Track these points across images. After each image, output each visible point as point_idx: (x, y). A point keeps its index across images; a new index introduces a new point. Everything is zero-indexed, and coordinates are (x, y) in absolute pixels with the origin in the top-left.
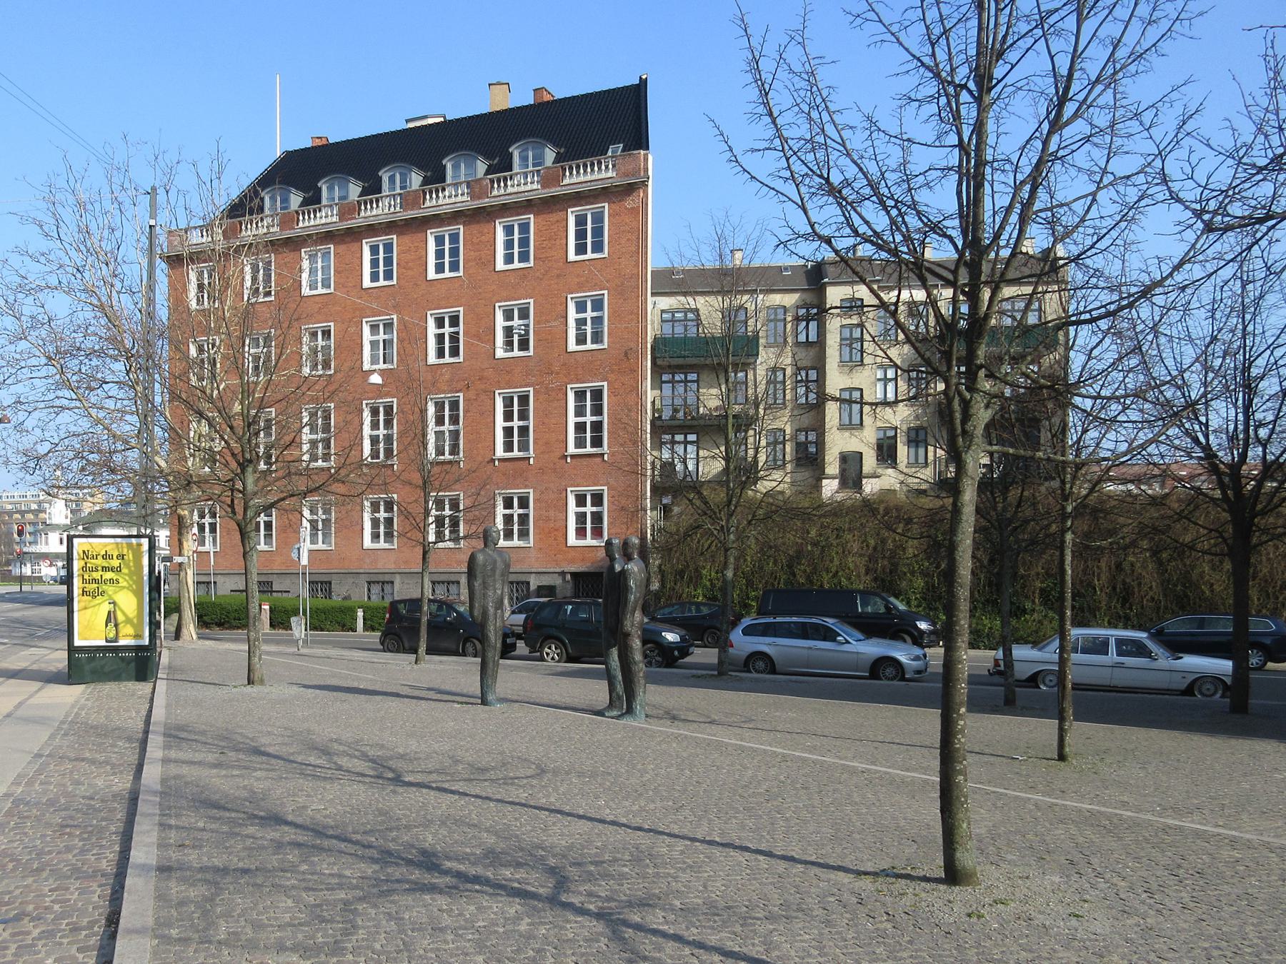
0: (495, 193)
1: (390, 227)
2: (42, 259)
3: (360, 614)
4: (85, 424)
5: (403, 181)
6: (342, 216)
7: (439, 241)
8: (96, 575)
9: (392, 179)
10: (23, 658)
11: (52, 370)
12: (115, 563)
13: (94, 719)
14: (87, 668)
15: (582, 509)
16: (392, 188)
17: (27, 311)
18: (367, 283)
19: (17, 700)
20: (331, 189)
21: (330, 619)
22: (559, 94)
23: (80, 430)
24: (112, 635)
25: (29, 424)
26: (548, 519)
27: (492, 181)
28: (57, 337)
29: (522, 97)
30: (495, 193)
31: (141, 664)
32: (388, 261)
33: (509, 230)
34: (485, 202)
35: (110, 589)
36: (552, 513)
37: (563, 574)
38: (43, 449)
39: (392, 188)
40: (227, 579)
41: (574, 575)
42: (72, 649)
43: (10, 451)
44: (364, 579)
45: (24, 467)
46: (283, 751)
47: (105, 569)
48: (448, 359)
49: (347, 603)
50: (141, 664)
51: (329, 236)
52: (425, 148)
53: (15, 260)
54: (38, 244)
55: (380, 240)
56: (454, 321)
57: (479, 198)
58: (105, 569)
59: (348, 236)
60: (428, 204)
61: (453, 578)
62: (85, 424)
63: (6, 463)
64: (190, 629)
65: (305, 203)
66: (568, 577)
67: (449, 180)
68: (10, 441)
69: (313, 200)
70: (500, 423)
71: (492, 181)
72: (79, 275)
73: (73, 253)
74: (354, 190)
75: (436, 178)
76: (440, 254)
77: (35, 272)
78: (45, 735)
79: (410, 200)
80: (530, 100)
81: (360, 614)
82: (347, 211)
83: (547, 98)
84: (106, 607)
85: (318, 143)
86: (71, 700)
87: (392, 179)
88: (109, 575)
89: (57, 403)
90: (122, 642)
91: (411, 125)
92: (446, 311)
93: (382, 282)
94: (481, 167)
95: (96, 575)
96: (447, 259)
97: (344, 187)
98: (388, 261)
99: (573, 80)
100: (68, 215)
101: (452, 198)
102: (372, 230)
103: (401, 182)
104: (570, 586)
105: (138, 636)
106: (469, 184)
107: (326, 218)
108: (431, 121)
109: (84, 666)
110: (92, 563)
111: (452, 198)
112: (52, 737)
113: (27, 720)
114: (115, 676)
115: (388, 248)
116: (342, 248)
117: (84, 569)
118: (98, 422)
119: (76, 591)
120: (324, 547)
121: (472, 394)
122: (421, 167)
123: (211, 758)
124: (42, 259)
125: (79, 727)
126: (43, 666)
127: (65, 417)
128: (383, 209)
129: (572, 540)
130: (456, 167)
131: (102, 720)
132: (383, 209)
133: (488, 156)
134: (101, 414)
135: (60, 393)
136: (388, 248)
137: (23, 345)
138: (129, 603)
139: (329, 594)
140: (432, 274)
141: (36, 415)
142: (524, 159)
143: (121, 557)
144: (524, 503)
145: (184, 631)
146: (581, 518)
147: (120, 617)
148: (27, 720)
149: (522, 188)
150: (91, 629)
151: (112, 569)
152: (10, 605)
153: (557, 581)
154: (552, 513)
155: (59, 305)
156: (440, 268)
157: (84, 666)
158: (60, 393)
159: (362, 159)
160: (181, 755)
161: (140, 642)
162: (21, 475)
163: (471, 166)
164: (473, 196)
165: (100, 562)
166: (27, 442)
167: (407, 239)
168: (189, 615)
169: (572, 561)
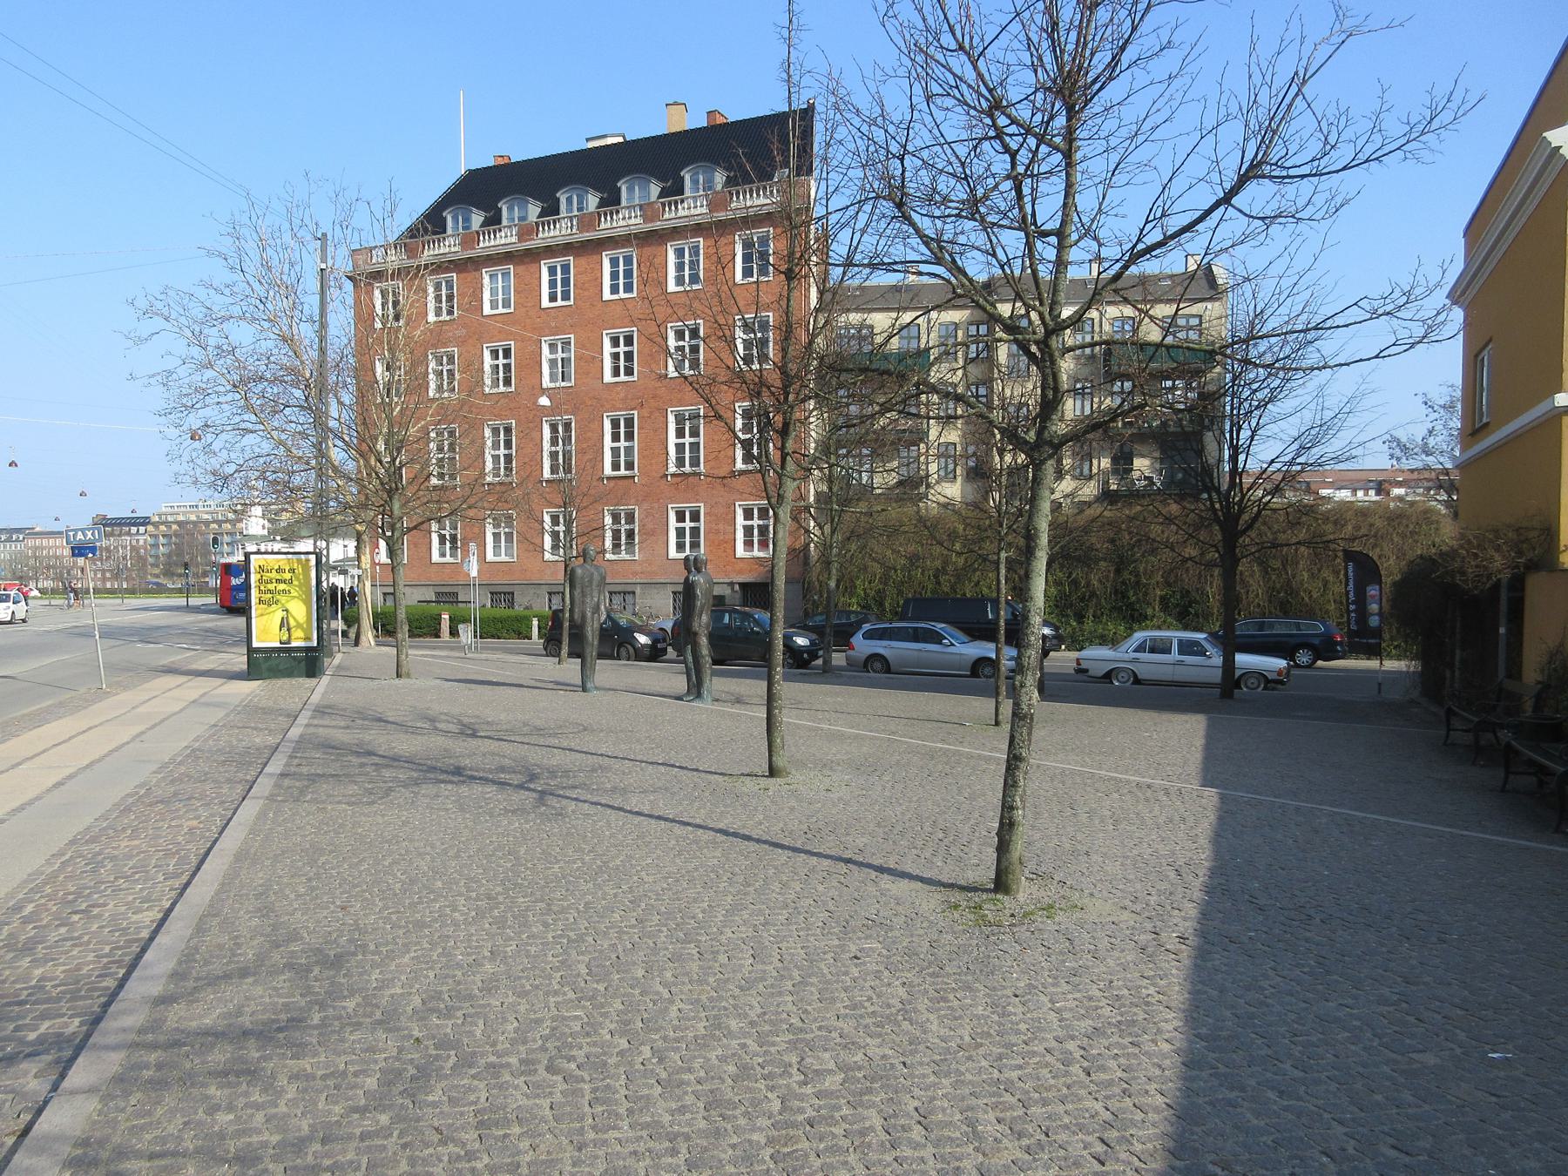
0: (667, 216)
1: (567, 248)
2: (227, 291)
3: (535, 622)
4: (266, 447)
5: (580, 202)
6: (522, 236)
7: (614, 262)
8: (271, 587)
9: (569, 200)
10: (212, 661)
11: (238, 396)
12: (287, 576)
13: (263, 704)
14: (264, 666)
15: (749, 523)
16: (570, 210)
17: (212, 342)
18: (545, 303)
19: (202, 691)
20: (510, 209)
21: (501, 626)
22: (733, 117)
23: (264, 452)
24: (285, 638)
25: (216, 446)
26: (718, 532)
27: (663, 205)
28: (241, 366)
29: (696, 120)
30: (667, 216)
31: (309, 662)
32: (566, 282)
33: (680, 253)
34: (657, 225)
35: (283, 598)
36: (721, 526)
37: (731, 584)
38: (231, 469)
39: (570, 210)
40: (415, 590)
41: (743, 585)
42: (251, 651)
43: (199, 471)
44: (545, 590)
45: (213, 485)
46: (398, 720)
47: (278, 581)
48: (623, 378)
49: (527, 613)
50: (309, 662)
51: (507, 257)
52: (601, 169)
53: (201, 293)
54: (222, 276)
55: (558, 261)
56: (629, 341)
57: (652, 221)
58: (278, 581)
59: (527, 257)
60: (603, 226)
61: (629, 588)
62: (266, 447)
63: (195, 482)
64: (368, 636)
65: (486, 223)
66: (737, 587)
67: (624, 203)
68: (199, 462)
69: (493, 221)
70: (672, 439)
71: (663, 205)
72: (261, 307)
73: (256, 286)
74: (534, 210)
75: (611, 201)
76: (614, 276)
77: (219, 303)
78: (221, 714)
79: (587, 222)
80: (702, 122)
81: (535, 622)
82: (526, 232)
83: (720, 120)
84: (280, 614)
85: (501, 161)
86: (247, 691)
87: (569, 200)
88: (282, 587)
89: (243, 426)
90: (294, 644)
91: (591, 145)
92: (621, 331)
93: (560, 303)
94: (655, 189)
95: (271, 587)
96: (621, 281)
97: (523, 207)
98: (566, 282)
99: (751, 98)
100: (251, 246)
101: (626, 220)
102: (550, 251)
103: (579, 202)
104: (738, 596)
105: (308, 639)
106: (641, 206)
107: (505, 238)
108: (610, 141)
109: (262, 664)
110: (267, 576)
111: (626, 220)
112: (227, 715)
113: (207, 705)
114: (289, 673)
115: (566, 269)
116: (521, 269)
117: (260, 581)
118: (281, 443)
119: (254, 601)
120: (507, 559)
121: (645, 413)
122: (596, 189)
123: (343, 724)
124: (227, 291)
125: (252, 712)
126: (229, 668)
127: (250, 439)
128: (561, 231)
129: (740, 551)
130: (630, 190)
131: (271, 703)
132: (561, 231)
133: (661, 179)
134: (283, 437)
135: (246, 417)
136: (566, 269)
137: (209, 374)
138: (299, 611)
139: (511, 604)
140: (607, 295)
141: (224, 436)
142: (695, 182)
143: (292, 571)
144: (695, 517)
145: (363, 638)
146: (748, 531)
147: (292, 623)
148: (207, 705)
149: (693, 212)
150: (266, 631)
151: (284, 582)
152: (204, 616)
153: (727, 591)
154: (721, 526)
155: (242, 335)
156: (614, 289)
157: (262, 664)
158: (246, 417)
159: (540, 180)
160: (321, 722)
161: (309, 644)
162: (209, 492)
163: (645, 189)
164: (646, 220)
165: (274, 575)
166: (214, 463)
167: (583, 261)
168: (367, 622)
169: (740, 572)
